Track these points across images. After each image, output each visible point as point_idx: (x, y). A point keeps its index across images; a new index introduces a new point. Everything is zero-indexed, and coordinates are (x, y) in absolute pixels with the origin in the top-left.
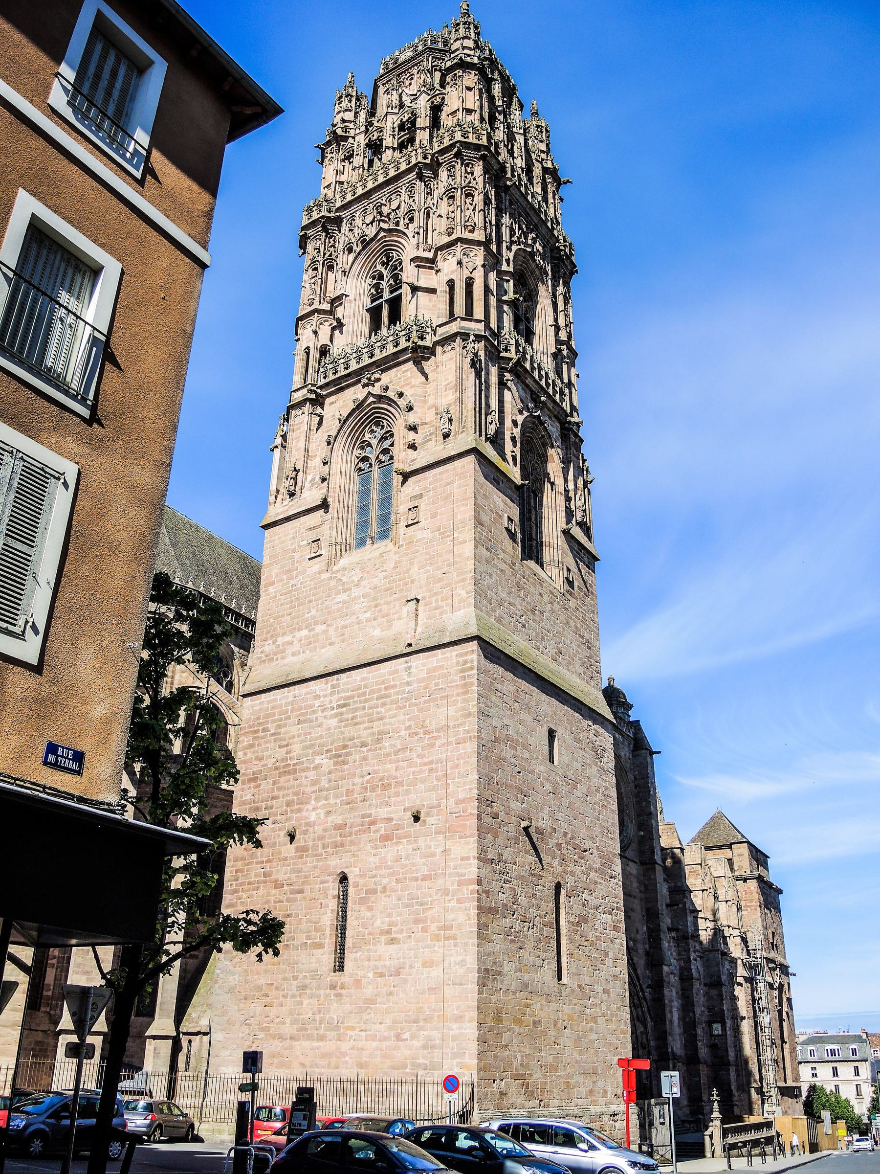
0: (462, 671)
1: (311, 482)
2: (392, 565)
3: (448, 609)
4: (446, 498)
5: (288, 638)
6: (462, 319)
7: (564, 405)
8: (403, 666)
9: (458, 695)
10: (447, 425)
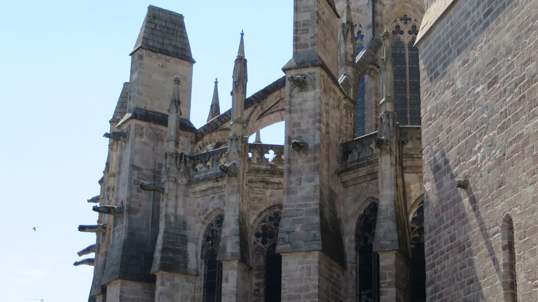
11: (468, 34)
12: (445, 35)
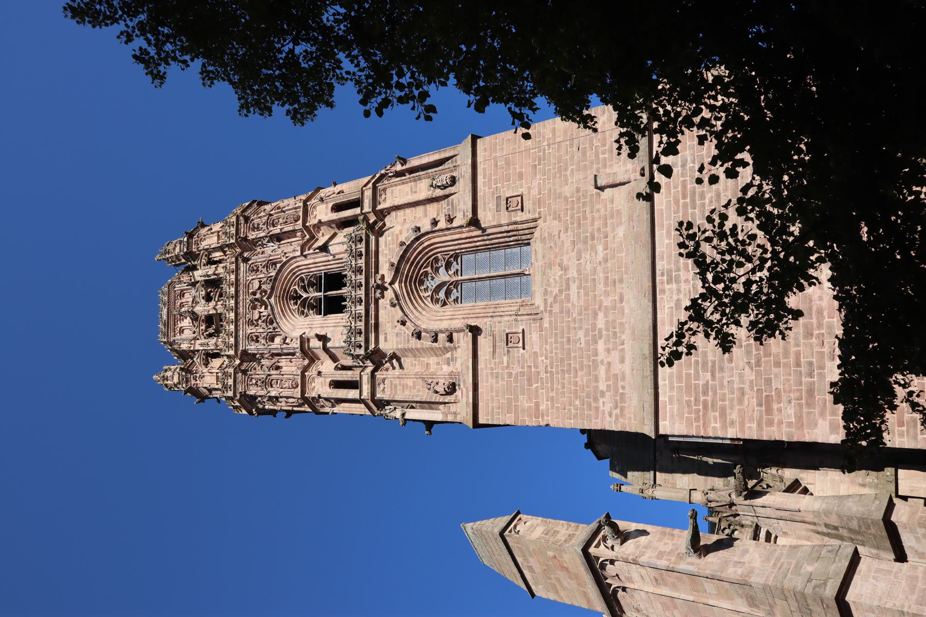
5: (602, 370)
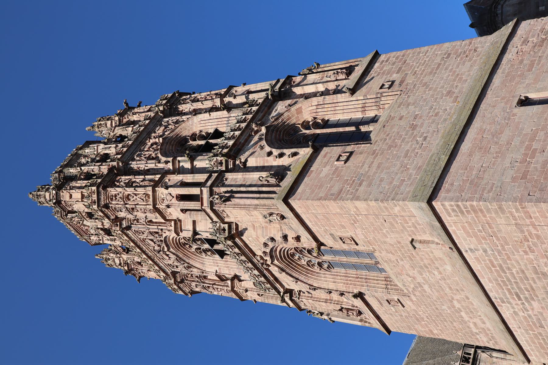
0: (462, 212)
1: (347, 299)
2: (390, 255)
3: (413, 220)
4: (327, 219)
5: (472, 325)
6: (202, 205)
7: (260, 101)
8: (470, 254)
9: (485, 216)
10: (275, 217)
11: (530, 316)
12: (526, 335)
